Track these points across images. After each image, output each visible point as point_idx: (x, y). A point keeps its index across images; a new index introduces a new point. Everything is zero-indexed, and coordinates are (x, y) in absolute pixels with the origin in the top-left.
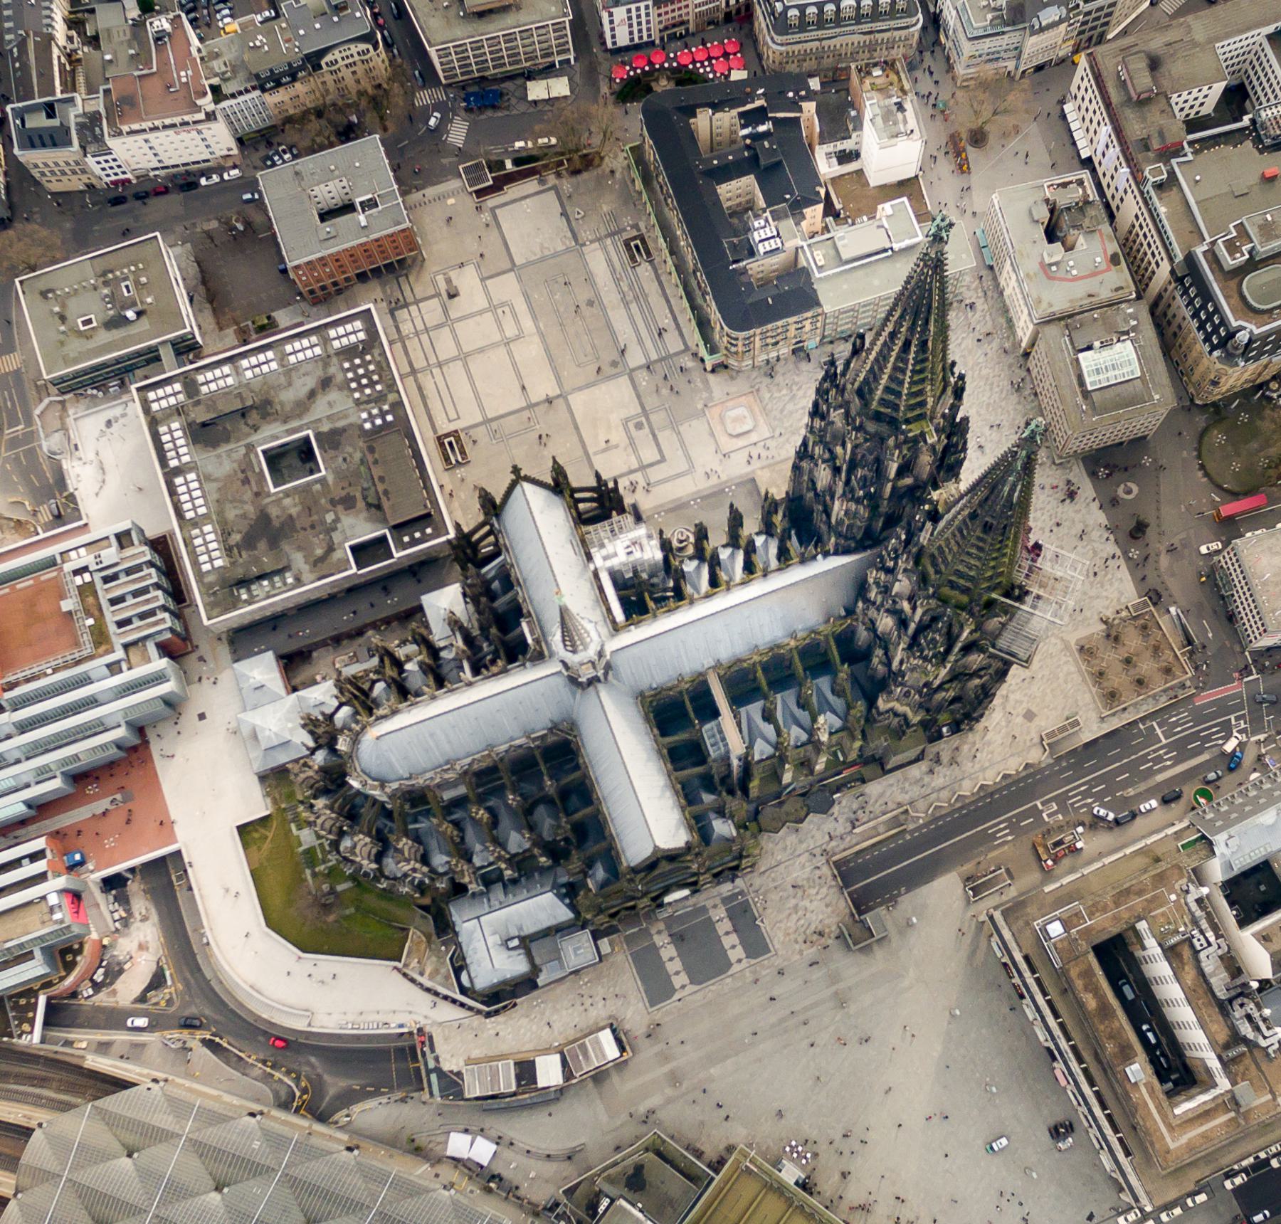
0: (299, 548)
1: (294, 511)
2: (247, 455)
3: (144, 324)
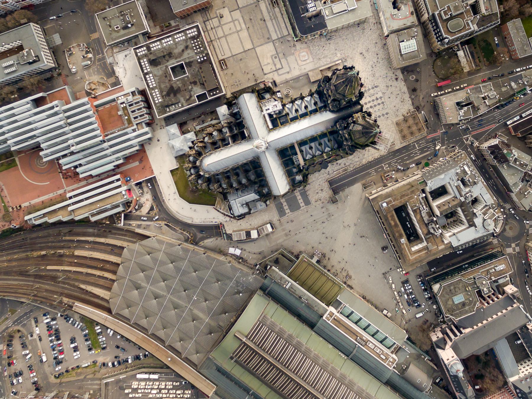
0: (182, 96)
1: (180, 85)
2: (166, 69)
3: (134, 28)
